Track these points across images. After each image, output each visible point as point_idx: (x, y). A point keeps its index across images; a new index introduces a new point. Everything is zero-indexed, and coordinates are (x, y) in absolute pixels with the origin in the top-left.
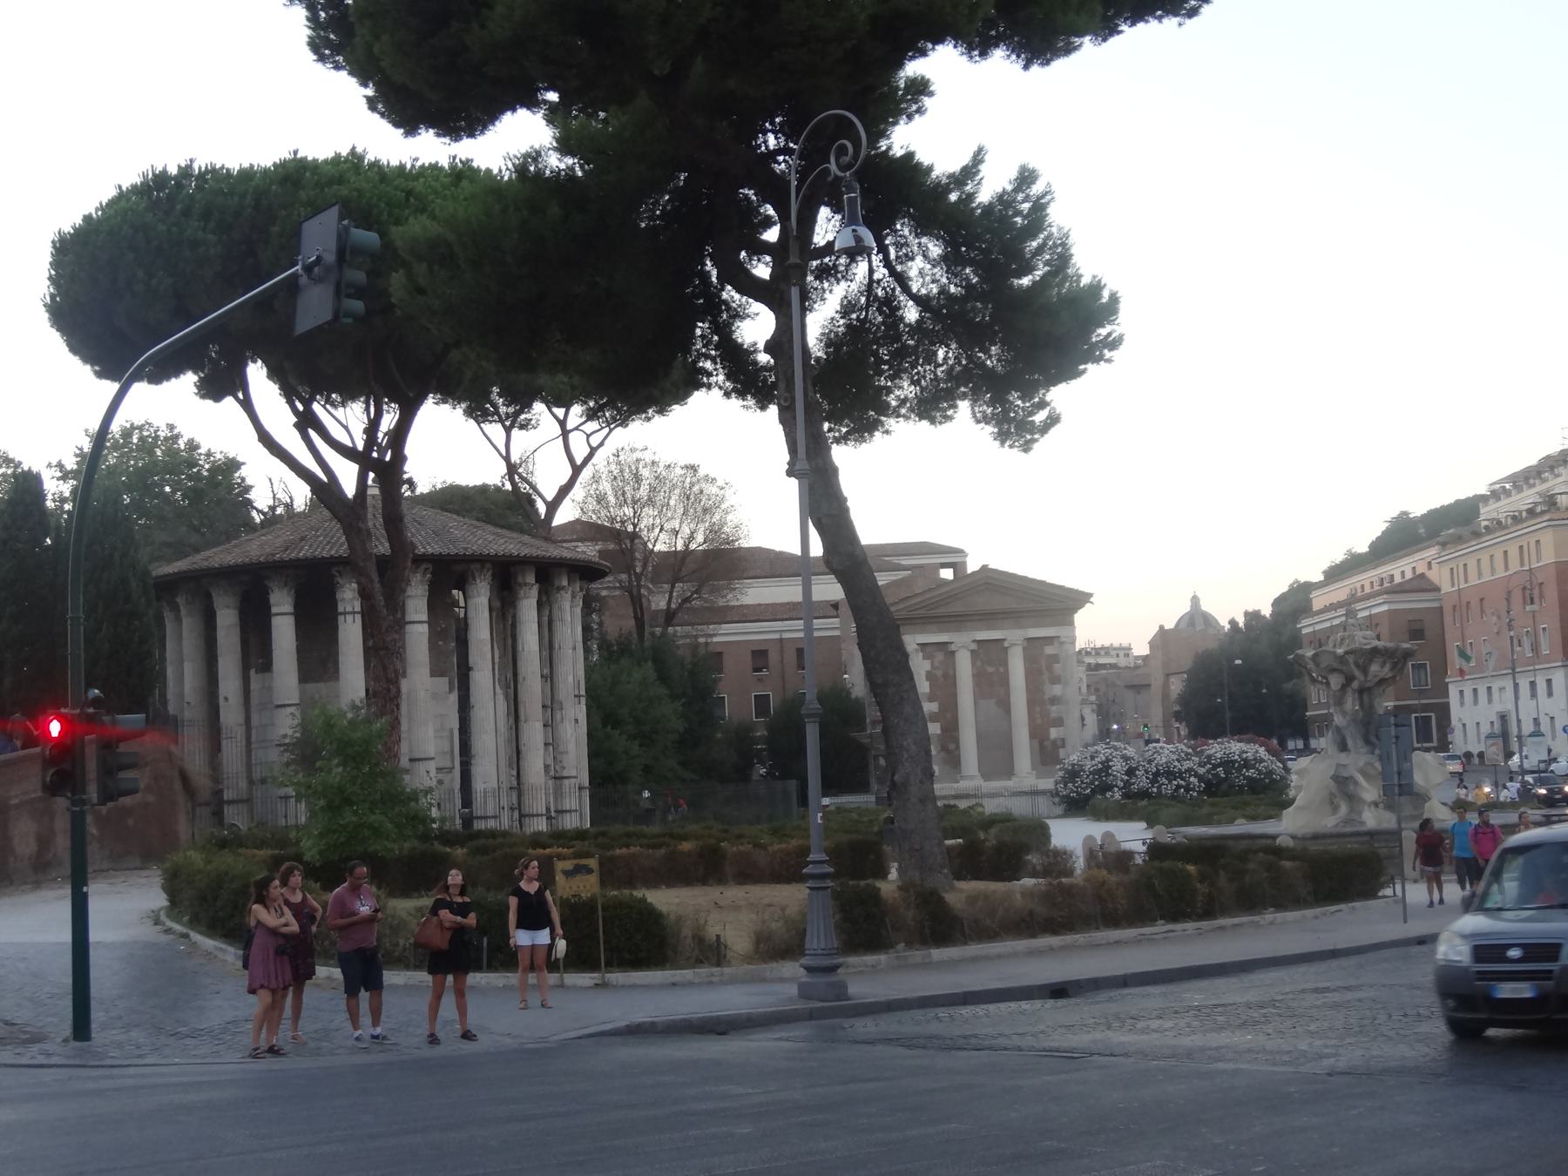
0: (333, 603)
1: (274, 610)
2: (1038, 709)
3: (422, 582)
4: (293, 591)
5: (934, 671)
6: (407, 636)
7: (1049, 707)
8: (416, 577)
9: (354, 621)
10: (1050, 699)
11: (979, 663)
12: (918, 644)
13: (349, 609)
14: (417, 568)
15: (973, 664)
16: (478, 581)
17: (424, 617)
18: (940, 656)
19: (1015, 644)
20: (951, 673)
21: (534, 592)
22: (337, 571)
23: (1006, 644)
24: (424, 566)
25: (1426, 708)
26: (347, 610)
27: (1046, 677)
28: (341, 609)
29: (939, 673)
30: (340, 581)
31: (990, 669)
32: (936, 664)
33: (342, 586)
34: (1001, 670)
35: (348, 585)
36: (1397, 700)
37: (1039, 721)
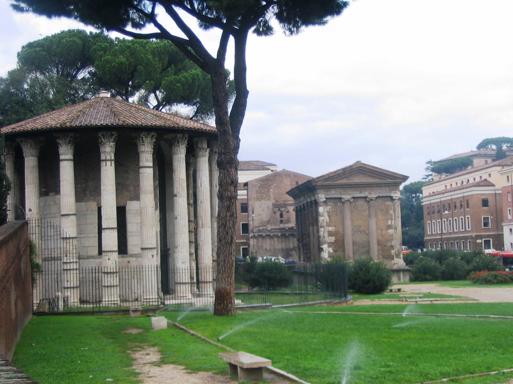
0: (98, 154)
1: (62, 157)
3: (150, 143)
4: (73, 146)
6: (141, 175)
8: (147, 140)
9: (111, 165)
13: (108, 158)
14: (148, 134)
16: (180, 144)
17: (151, 164)
19: (372, 200)
21: (207, 154)
22: (101, 135)
24: (153, 133)
25: (489, 236)
26: (107, 158)
28: (103, 157)
30: (103, 140)
33: (104, 144)
35: (108, 143)
36: (477, 232)
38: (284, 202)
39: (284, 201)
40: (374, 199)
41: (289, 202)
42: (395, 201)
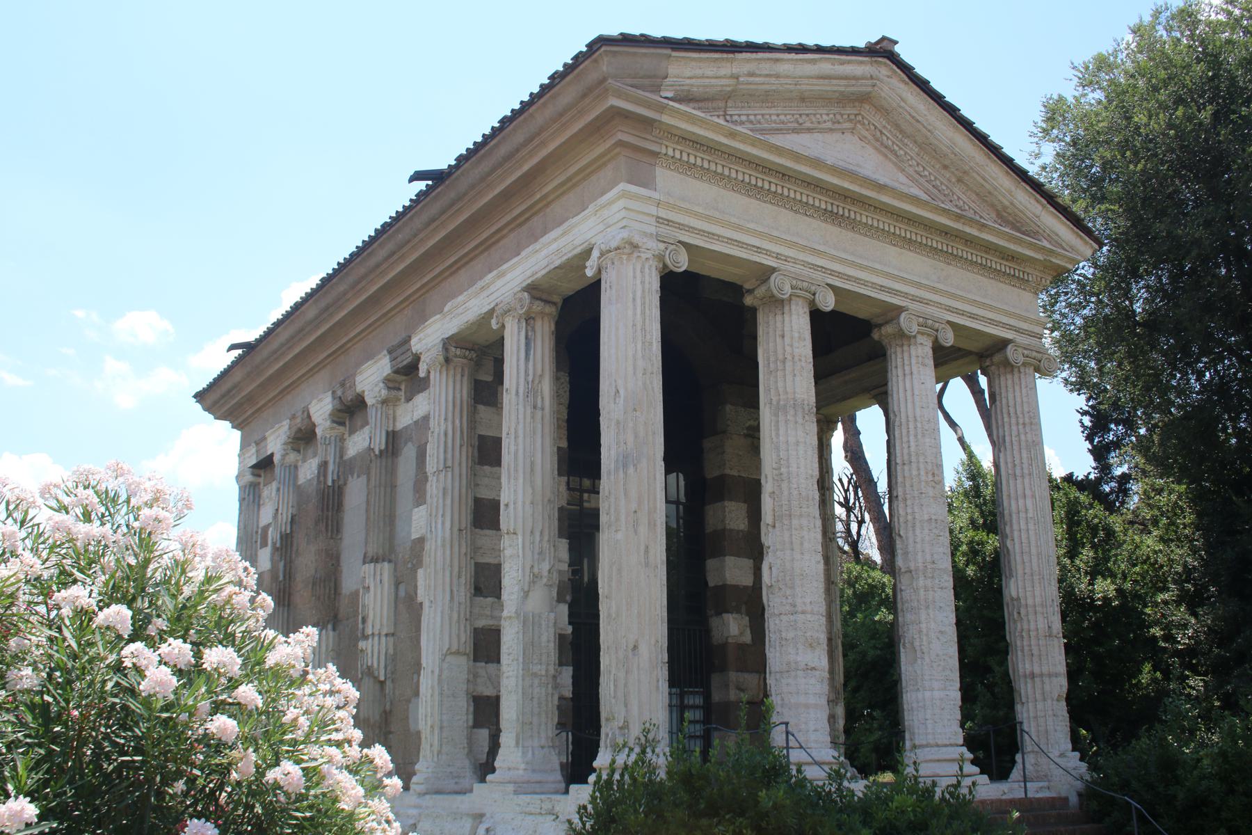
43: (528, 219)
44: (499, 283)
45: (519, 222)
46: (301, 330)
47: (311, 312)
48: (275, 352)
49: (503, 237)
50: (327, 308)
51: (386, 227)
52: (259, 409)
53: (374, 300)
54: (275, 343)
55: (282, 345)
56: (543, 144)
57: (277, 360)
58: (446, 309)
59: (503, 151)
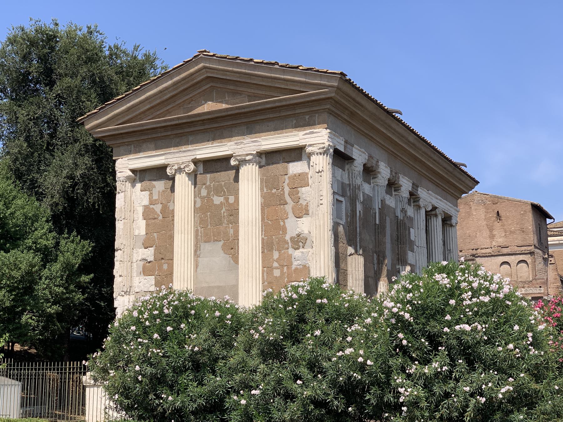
2: (276, 255)
5: (152, 206)
7: (291, 251)
10: (292, 238)
11: (204, 192)
12: (133, 171)
15: (197, 194)
18: (160, 185)
20: (171, 208)
23: (233, 162)
27: (289, 208)
29: (158, 208)
31: (218, 200)
32: (155, 197)
34: (232, 199)
37: (277, 273)
38: (474, 252)
39: (473, 250)
40: (248, 158)
41: (484, 251)
42: (313, 158)
43: (444, 191)
44: (439, 202)
45: (444, 190)
46: (403, 136)
47: (411, 138)
48: (390, 126)
49: (440, 188)
50: (414, 145)
51: (425, 142)
52: (350, 123)
53: (416, 159)
54: (394, 125)
55: (395, 130)
56: (461, 184)
57: (386, 129)
58: (430, 192)
59: (464, 179)
